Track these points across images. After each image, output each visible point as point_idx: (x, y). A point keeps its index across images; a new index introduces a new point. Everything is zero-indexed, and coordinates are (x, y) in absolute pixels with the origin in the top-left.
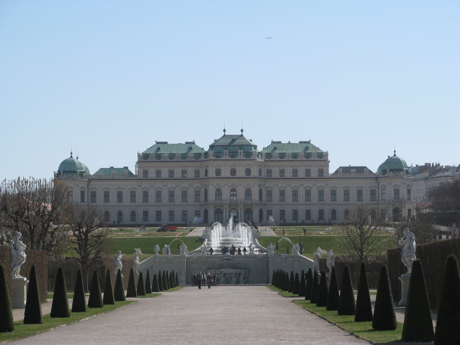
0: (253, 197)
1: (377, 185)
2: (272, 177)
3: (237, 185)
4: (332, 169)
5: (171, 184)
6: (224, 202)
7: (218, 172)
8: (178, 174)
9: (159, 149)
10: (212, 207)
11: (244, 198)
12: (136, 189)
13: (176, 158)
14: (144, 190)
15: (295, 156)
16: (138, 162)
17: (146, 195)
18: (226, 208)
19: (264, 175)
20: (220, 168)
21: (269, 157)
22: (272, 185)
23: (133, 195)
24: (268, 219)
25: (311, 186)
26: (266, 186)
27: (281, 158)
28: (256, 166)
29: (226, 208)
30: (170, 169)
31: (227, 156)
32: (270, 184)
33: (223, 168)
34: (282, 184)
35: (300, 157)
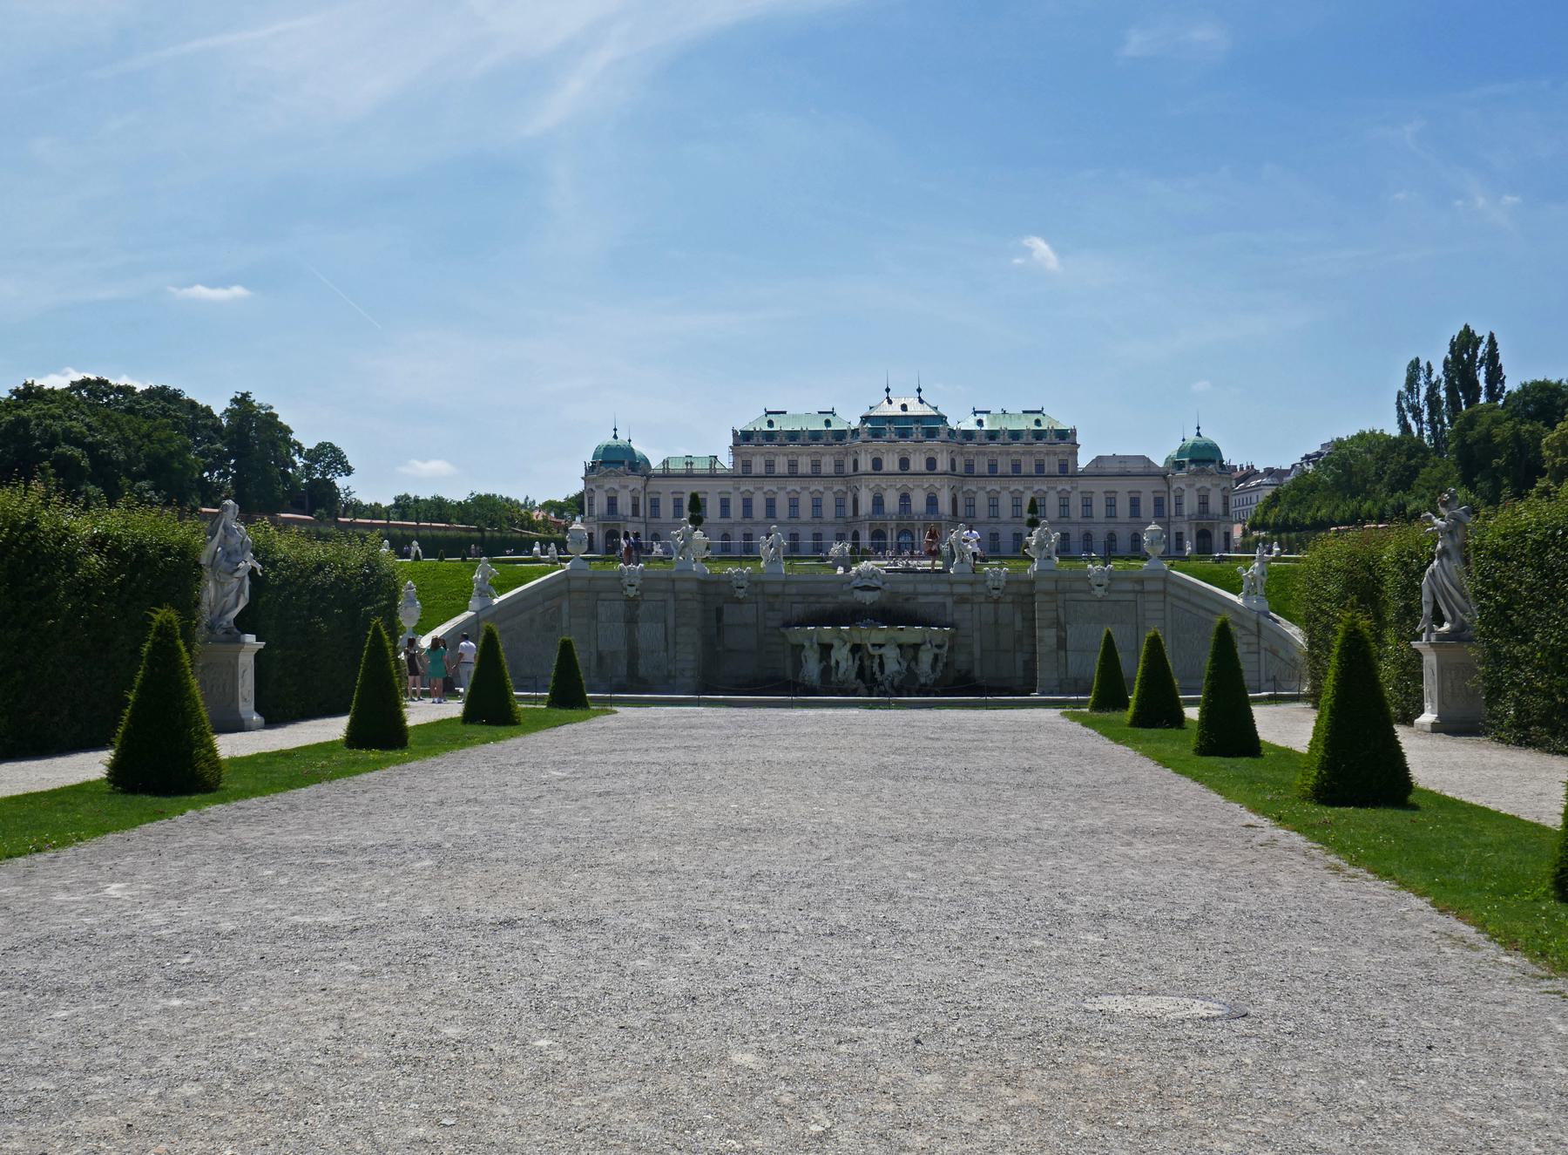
4: (1083, 461)
5: (793, 485)
7: (877, 463)
9: (770, 423)
15: (1015, 435)
17: (747, 505)
19: (960, 468)
32: (971, 485)
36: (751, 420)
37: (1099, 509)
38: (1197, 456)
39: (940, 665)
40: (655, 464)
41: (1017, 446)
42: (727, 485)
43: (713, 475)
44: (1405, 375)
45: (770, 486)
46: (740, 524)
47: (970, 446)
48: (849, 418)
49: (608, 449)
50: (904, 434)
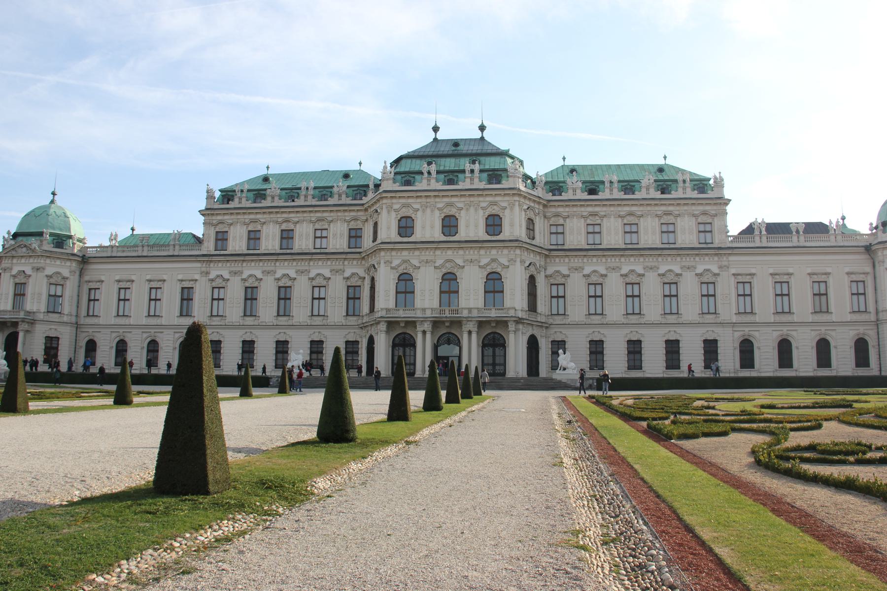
0: (508, 303)
1: (868, 269)
2: (565, 247)
3: (460, 262)
4: (735, 222)
6: (419, 314)
7: (406, 226)
8: (303, 240)
9: (266, 179)
10: (383, 327)
11: (480, 304)
12: (196, 280)
13: (302, 198)
14: (214, 284)
15: (629, 187)
18: (424, 332)
21: (557, 193)
22: (565, 271)
24: (555, 366)
25: (678, 271)
26: (550, 270)
27: (592, 192)
28: (517, 208)
29: (424, 332)
30: (284, 227)
31: (433, 181)
32: (561, 266)
33: (419, 213)
35: (644, 190)
42: (191, 271)
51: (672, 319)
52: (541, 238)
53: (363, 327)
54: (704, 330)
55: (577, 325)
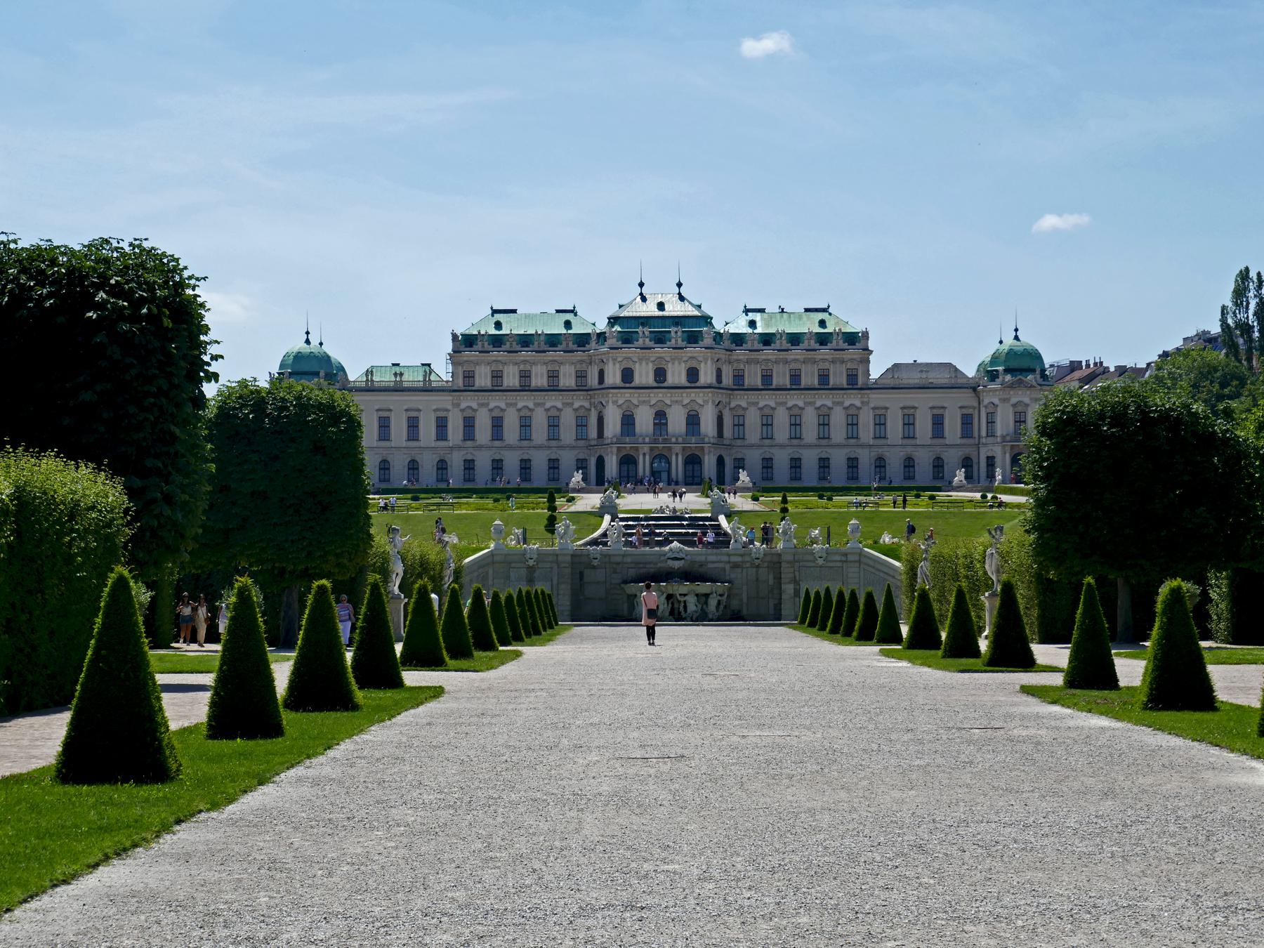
1: (976, 404)
3: (668, 402)
4: (876, 370)
5: (525, 401)
7: (627, 375)
9: (498, 325)
10: (615, 450)
12: (447, 410)
15: (795, 339)
16: (455, 356)
17: (469, 424)
19: (727, 380)
20: (630, 365)
22: (744, 404)
23: (442, 425)
25: (829, 403)
26: (733, 405)
30: (522, 367)
32: (741, 400)
34: (767, 400)
36: (474, 320)
37: (895, 428)
38: (1014, 364)
39: (722, 607)
40: (355, 374)
41: (797, 353)
42: (445, 401)
43: (427, 388)
44: (1232, 286)
45: (497, 401)
46: (460, 448)
47: (740, 353)
48: (594, 319)
49: (299, 357)
50: (660, 339)
51: (824, 442)
52: (727, 380)
53: (589, 447)
54: (846, 451)
55: (752, 446)
